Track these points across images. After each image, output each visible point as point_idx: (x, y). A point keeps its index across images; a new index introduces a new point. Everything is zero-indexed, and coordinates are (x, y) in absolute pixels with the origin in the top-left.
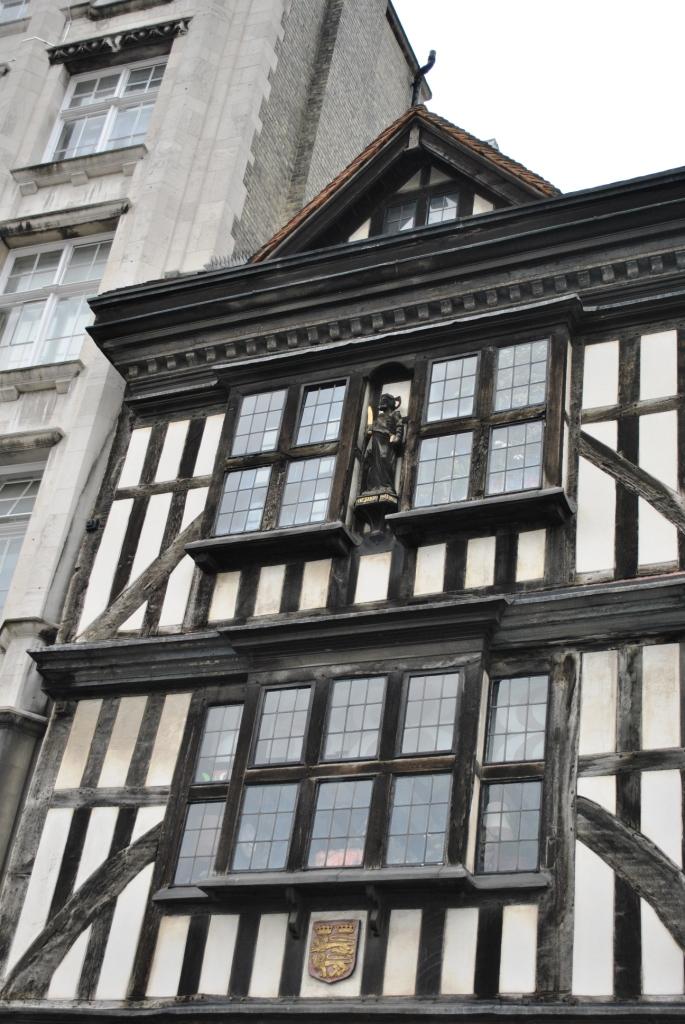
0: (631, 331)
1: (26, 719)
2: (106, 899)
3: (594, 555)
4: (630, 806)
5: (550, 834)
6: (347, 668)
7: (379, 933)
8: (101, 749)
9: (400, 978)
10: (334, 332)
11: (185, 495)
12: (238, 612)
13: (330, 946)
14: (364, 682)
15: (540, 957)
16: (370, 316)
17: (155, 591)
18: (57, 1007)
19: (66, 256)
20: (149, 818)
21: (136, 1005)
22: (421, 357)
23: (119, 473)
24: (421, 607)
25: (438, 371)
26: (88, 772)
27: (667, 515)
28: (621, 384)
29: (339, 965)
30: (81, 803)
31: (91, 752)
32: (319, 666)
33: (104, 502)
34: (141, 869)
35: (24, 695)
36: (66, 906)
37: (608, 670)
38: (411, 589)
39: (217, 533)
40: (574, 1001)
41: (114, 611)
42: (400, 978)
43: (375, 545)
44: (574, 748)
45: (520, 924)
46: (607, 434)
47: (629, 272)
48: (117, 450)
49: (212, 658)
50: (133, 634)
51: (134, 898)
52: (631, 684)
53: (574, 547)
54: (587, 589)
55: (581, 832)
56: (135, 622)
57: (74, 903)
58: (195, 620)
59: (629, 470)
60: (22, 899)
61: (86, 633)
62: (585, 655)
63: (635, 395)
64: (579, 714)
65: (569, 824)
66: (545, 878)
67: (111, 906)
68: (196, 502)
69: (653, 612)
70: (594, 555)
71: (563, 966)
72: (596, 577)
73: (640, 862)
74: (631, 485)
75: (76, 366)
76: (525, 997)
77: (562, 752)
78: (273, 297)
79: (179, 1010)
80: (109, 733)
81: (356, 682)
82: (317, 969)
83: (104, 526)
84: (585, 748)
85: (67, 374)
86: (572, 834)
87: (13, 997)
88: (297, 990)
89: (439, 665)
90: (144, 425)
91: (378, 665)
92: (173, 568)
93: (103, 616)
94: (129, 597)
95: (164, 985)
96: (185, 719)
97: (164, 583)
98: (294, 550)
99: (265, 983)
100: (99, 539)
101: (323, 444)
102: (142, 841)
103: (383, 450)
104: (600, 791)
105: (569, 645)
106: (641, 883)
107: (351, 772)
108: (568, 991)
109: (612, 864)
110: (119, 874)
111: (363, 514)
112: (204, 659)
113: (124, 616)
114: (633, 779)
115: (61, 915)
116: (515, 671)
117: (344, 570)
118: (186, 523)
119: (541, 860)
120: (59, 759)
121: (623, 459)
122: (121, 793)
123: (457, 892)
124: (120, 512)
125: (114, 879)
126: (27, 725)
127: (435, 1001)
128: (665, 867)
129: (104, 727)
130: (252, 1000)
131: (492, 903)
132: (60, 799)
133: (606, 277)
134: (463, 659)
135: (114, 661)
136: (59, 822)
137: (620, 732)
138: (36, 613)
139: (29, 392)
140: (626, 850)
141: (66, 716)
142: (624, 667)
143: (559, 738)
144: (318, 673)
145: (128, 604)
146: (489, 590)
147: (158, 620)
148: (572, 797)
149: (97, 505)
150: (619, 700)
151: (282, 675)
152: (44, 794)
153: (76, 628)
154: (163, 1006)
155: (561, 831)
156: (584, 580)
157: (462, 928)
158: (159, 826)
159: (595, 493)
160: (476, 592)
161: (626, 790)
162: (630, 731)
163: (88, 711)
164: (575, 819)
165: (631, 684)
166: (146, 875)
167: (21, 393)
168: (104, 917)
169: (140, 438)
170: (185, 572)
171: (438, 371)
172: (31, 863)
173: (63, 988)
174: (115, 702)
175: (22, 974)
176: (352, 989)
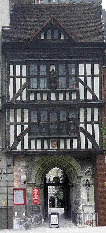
9: (62, 146)
17: (20, 93)
20: (26, 127)
29: (55, 146)
30: (15, 124)
34: (26, 133)
41: (15, 97)
42: (62, 146)
43: (53, 92)
44: (80, 121)
45: (75, 141)
48: (8, 69)
56: (19, 99)
61: (11, 100)
62: (80, 109)
66: (77, 136)
68: (24, 80)
70: (82, 97)
82: (52, 146)
95: (33, 146)
98: (42, 92)
99: (46, 147)
104: (83, 126)
118: (23, 84)
121: (85, 83)
123: (68, 138)
124: (11, 80)
132: (12, 124)
133: (82, 54)
137: (85, 119)
141: (9, 111)
143: (78, 119)
152: (9, 123)
159: (82, 88)
162: (86, 119)
163: (12, 111)
169: (11, 67)
170: (24, 92)
176: (57, 148)
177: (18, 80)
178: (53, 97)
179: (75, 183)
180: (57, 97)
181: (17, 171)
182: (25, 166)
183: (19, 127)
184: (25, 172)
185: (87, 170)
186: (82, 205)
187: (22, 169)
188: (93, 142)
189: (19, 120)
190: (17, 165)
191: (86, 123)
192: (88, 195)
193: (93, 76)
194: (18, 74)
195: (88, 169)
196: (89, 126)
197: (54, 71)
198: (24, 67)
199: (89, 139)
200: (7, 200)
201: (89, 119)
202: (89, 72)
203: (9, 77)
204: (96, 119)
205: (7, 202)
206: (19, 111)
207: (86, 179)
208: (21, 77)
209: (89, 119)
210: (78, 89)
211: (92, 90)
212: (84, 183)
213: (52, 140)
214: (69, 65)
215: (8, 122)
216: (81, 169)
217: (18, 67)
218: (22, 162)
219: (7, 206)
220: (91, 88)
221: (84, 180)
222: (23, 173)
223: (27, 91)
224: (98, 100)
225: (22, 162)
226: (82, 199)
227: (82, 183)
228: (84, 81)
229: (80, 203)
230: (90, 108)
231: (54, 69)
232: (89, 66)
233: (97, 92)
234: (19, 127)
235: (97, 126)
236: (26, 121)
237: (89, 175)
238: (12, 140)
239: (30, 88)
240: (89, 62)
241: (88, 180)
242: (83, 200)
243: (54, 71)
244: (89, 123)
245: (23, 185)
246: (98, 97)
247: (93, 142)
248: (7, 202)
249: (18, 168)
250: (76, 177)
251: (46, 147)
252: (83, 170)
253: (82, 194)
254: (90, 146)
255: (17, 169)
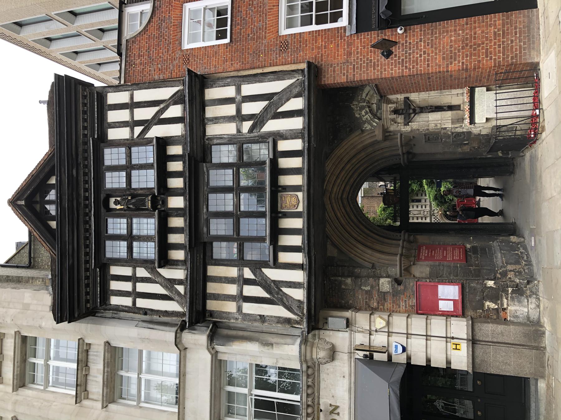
0: (106, 125)
1: (211, 330)
2: (272, 284)
3: (176, 130)
4: (250, 117)
5: (258, 139)
6: (205, 207)
7: (286, 188)
8: (224, 296)
9: (296, 180)
10: (88, 227)
11: (138, 277)
12: (181, 249)
13: (288, 203)
14: (209, 201)
15: (292, 139)
16: (84, 229)
17: (170, 283)
18: (305, 296)
19: (33, 360)
20: (248, 274)
21: (305, 267)
22: (103, 192)
23: (126, 307)
24: (187, 186)
25: (108, 186)
26: (231, 300)
27: (167, 109)
28: (122, 127)
30: (241, 300)
31: (224, 300)
32: (204, 216)
33: (136, 311)
35: (202, 332)
36: (274, 299)
37: (212, 127)
38: (181, 189)
39: (154, 258)
40: (304, 128)
41: (177, 298)
42: (296, 180)
43: (165, 202)
46: (138, 130)
47: (86, 125)
48: (118, 309)
49: (197, 257)
50: (185, 289)
51: (273, 274)
52: (216, 120)
53: (173, 137)
54: (187, 132)
55: (258, 131)
56: (181, 289)
57: (274, 296)
58: (183, 265)
59: (151, 122)
60: (271, 317)
63: (127, 122)
64: (224, 135)
65: (256, 134)
66: (270, 140)
67: (274, 281)
68: (142, 272)
69: (196, 112)
70: (176, 130)
71: (295, 132)
72: (183, 129)
73: (267, 113)
74: (156, 121)
75: (81, 341)
76: (303, 142)
77: (235, 138)
78: (71, 247)
79: (306, 251)
80: (218, 294)
81: (210, 203)
83: (145, 309)
84: (234, 131)
85: (83, 344)
86: (258, 133)
87: (303, 313)
88: (301, 212)
89: (206, 176)
90: (109, 299)
91: (205, 197)
92: (164, 277)
93: (178, 302)
94: (172, 293)
95: (298, 258)
96: (216, 267)
97: (170, 280)
100: (149, 309)
101: (127, 223)
102: (255, 275)
103: (133, 201)
104: (247, 126)
105: (203, 139)
106: (273, 112)
107: (237, 200)
108: (301, 130)
109: (267, 121)
110: (265, 281)
111: (154, 207)
112: (197, 259)
113: (178, 293)
114: (244, 117)
115: (278, 300)
116: (210, 155)
117: (172, 213)
119: (265, 142)
120: (226, 313)
121: (147, 124)
122: (239, 286)
123: (274, 163)
124: (141, 303)
125: (266, 282)
126: (213, 330)
127: (304, 168)
128: (268, 106)
129: (217, 297)
130: (303, 227)
131: (277, 154)
132: (239, 309)
134: (205, 169)
135: (194, 293)
136: (248, 308)
138: (173, 334)
139: (87, 362)
140: (263, 117)
141: (212, 314)
142: (211, 123)
143: (230, 140)
144: (205, 217)
145: (174, 293)
146: (184, 163)
147: (182, 280)
148: (248, 134)
149: (137, 313)
150: (221, 123)
151: (205, 230)
152: (237, 316)
153: (181, 312)
154: (305, 257)
155: (258, 136)
156: (184, 133)
157: (285, 163)
158: (250, 269)
159: (157, 131)
160: (184, 167)
161: (247, 118)
163: (212, 305)
164: (254, 133)
165: (216, 120)
166: (266, 271)
167: (87, 366)
168: (278, 284)
169: (115, 301)
170: (167, 273)
171: (108, 186)
172: (260, 315)
173: (299, 294)
174: (208, 295)
175: (296, 311)
176: (300, 195)
177: (141, 287)
178: (176, 202)
179: (402, 146)
180: (175, 192)
181: (366, 302)
182: (355, 278)
183: (250, 291)
184: (371, 279)
185: (366, 115)
186: (468, 124)
187: (363, 288)
188: (286, 95)
189: (232, 290)
190: (351, 302)
191: (240, 117)
192: (438, 108)
193: (132, 106)
194: (127, 286)
195: (363, 113)
196: (250, 108)
197: (119, 199)
198: (115, 270)
199: (279, 108)
200: (446, 337)
201: (230, 110)
202: (123, 115)
203: (134, 309)
204: (229, 92)
205: (453, 338)
206: (212, 288)
207: (389, 116)
208: (133, 279)
209: (230, 110)
210: (155, 140)
211: (162, 106)
212: (402, 121)
213: (279, 205)
214: (107, 162)
215: (237, 319)
216: (363, 131)
217: (115, 285)
218: (343, 287)
219: (468, 340)
220: (155, 109)
221: (392, 123)
222: (374, 283)
223: (160, 266)
224: (183, 87)
225: (343, 287)
226: (449, 125)
227: (402, 127)
228: (142, 127)
229: (459, 130)
230: (206, 108)
231: (115, 199)
232: (113, 116)
233: (166, 93)
234: (250, 291)
235: (248, 89)
236: (233, 272)
237: (379, 108)
238: (280, 311)
239: (152, 262)
240: (102, 117)
241: (396, 112)
242: (453, 123)
243: (119, 199)
244: (239, 110)
245: (405, 287)
246: (175, 89)
247: (286, 95)
248: (453, 338)
249: (360, 297)
250: (387, 143)
251: (298, 223)
252: (366, 125)
253: (436, 126)
254: (297, 104)
255: (363, 301)
